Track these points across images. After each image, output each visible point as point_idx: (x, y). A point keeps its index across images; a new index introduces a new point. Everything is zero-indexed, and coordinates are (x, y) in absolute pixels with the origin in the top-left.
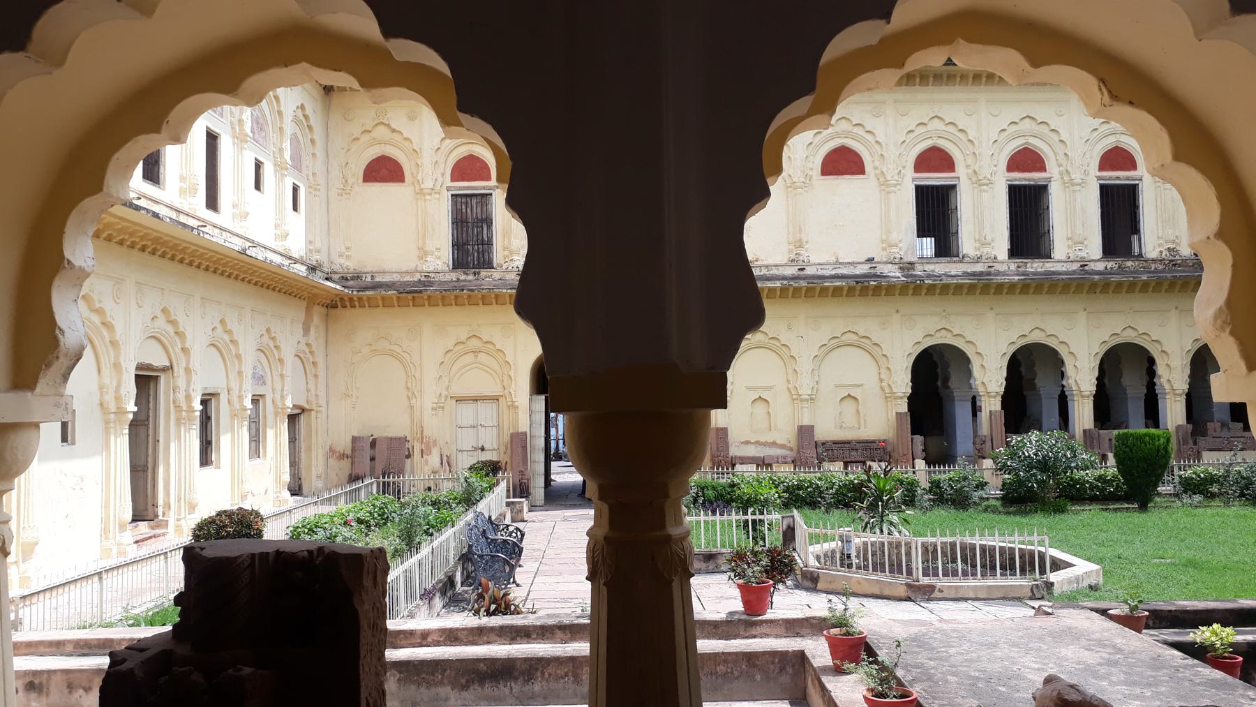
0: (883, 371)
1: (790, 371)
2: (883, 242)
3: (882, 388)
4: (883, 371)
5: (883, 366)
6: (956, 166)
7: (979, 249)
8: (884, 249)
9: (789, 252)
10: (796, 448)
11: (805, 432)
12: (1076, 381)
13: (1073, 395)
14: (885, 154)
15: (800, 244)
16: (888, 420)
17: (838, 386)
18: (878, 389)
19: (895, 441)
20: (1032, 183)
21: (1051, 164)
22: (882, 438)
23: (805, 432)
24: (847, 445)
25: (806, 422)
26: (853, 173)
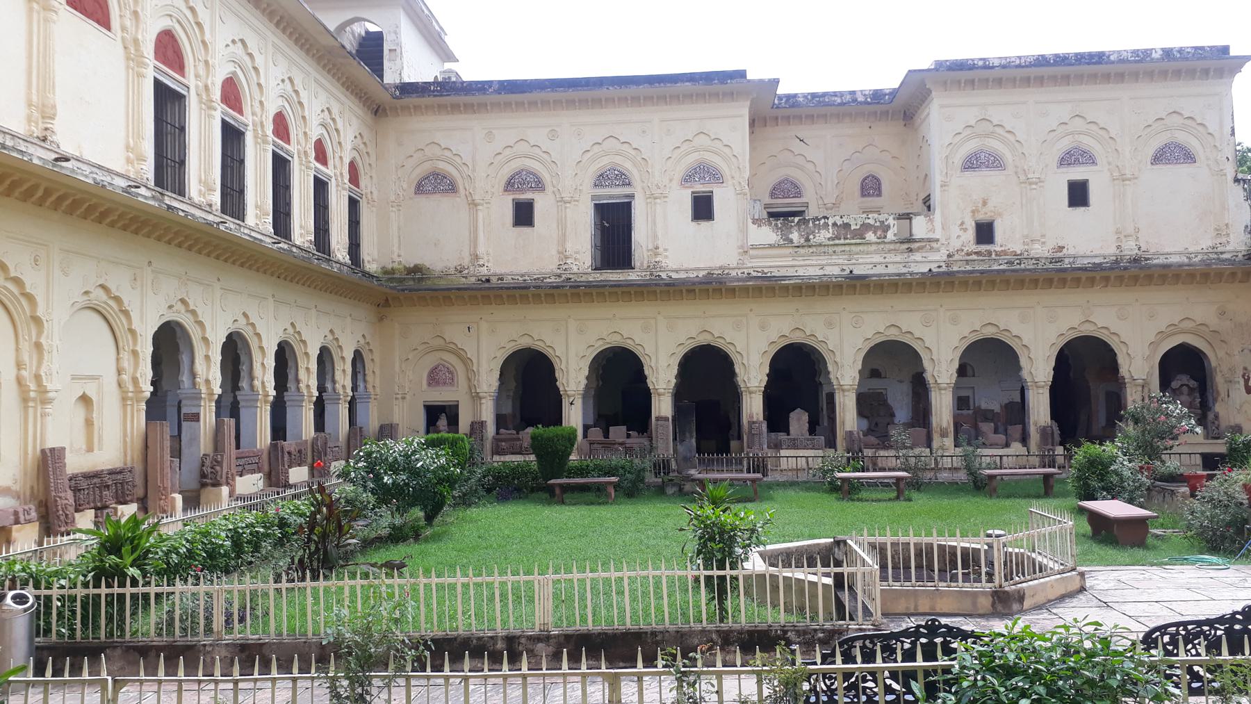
0: (125, 356)
1: (26, 346)
2: (128, 148)
3: (120, 385)
4: (125, 356)
5: (126, 348)
6: (187, 70)
7: (204, 196)
8: (128, 161)
9: (29, 119)
10: (28, 493)
11: (49, 461)
12: (263, 383)
13: (257, 400)
14: (139, 10)
15: (47, 113)
16: (125, 435)
17: (74, 378)
18: (115, 385)
19: (139, 468)
20: (237, 125)
21: (247, 109)
22: (118, 464)
23: (49, 461)
24: (96, 480)
25: (50, 444)
26: (98, 22)
